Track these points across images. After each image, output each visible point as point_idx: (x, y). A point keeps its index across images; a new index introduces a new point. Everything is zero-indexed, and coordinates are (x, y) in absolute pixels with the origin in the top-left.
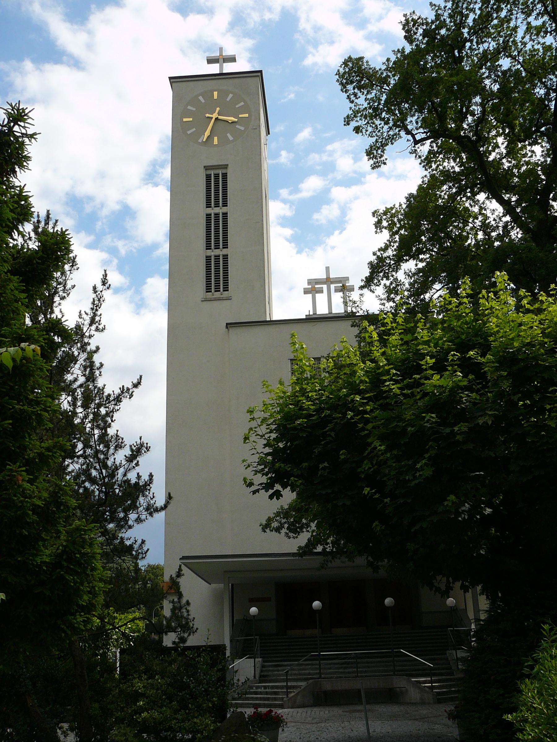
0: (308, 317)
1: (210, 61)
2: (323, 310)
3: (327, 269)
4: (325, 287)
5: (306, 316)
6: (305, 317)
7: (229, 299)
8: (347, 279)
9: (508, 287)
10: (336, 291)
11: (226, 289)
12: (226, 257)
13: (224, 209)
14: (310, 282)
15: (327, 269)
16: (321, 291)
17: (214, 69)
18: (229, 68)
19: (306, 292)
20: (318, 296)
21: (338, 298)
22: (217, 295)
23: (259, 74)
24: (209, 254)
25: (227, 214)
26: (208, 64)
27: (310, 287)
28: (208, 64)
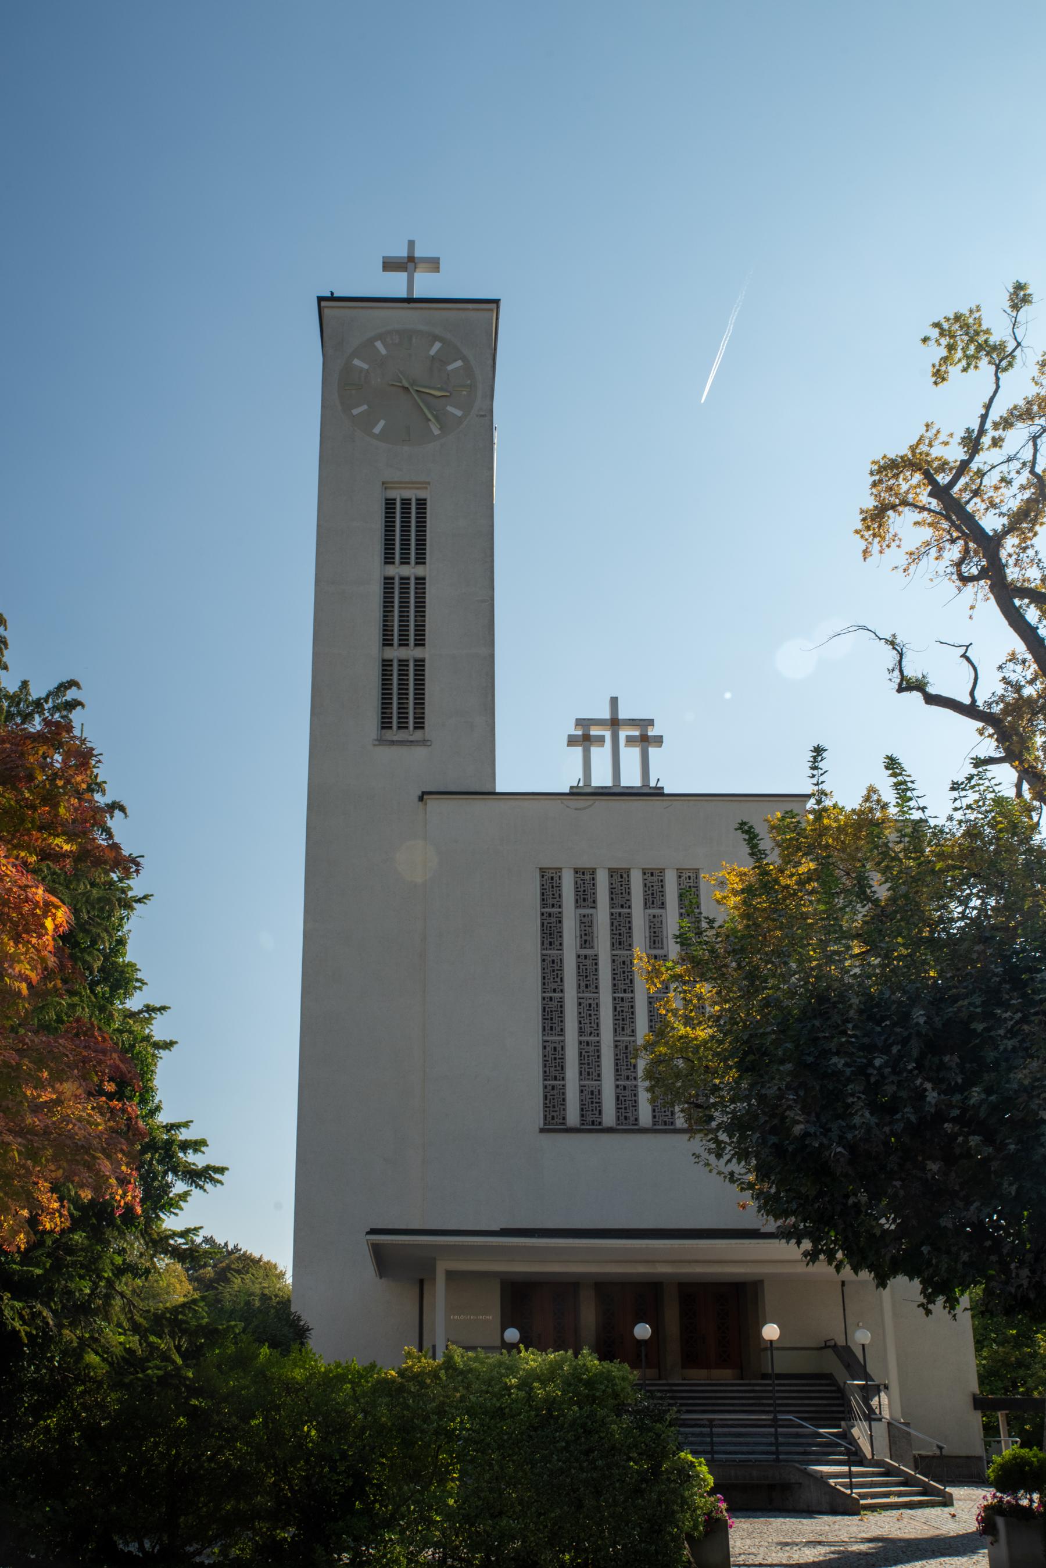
0: (575, 790)
1: (390, 265)
2: (601, 778)
3: (614, 701)
4: (608, 735)
5: (572, 788)
6: (567, 791)
7: (424, 742)
8: (651, 722)
9: (88, 825)
10: (630, 740)
11: (419, 725)
12: (420, 664)
13: (420, 571)
14: (580, 722)
15: (614, 701)
16: (601, 740)
17: (395, 285)
18: (426, 285)
19: (572, 741)
20: (595, 751)
21: (630, 756)
22: (402, 735)
23: (494, 306)
24: (419, 649)
25: (424, 579)
26: (439, 258)
27: (580, 733)
28: (439, 258)
